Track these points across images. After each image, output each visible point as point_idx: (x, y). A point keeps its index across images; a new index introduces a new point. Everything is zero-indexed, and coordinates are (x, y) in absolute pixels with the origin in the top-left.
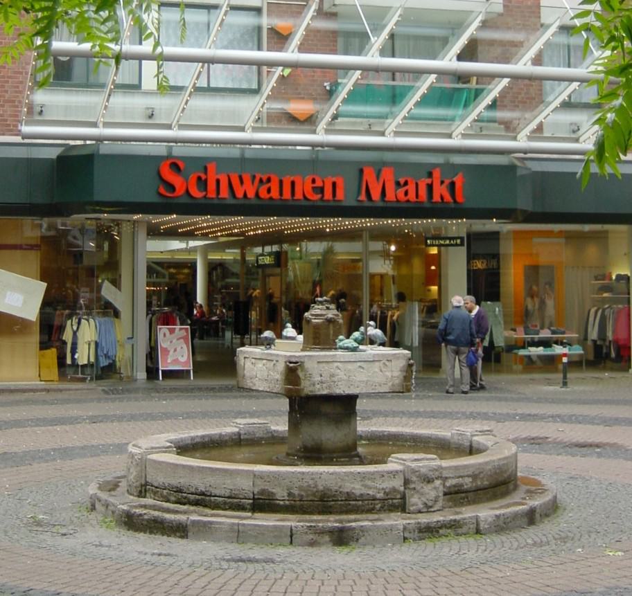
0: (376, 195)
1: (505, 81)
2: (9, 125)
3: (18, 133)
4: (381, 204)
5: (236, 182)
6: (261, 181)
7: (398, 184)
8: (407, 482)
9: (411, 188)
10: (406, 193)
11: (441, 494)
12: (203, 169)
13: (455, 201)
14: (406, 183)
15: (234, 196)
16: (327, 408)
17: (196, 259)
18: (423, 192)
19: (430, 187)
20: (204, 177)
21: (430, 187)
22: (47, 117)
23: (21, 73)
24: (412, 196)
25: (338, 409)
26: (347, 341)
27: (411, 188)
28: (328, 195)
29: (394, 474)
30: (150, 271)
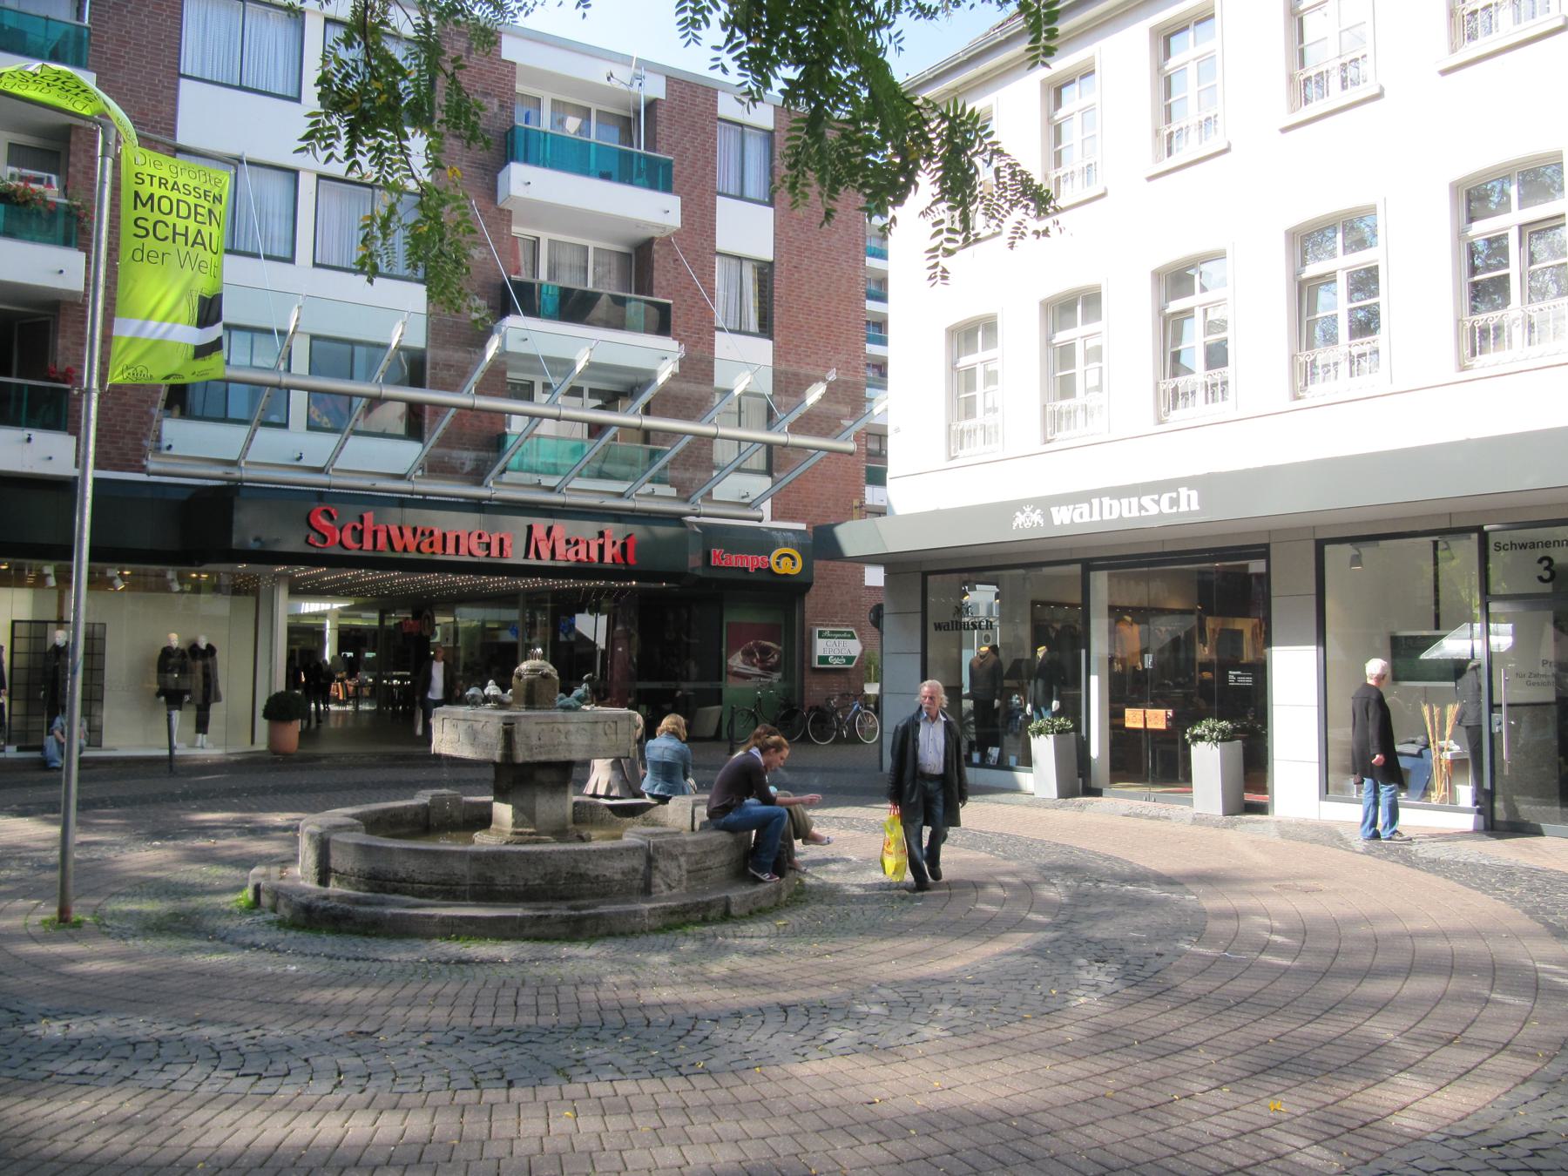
0: (546, 554)
1: (688, 438)
2: (129, 460)
3: (142, 469)
4: (551, 563)
5: (395, 533)
6: (423, 534)
7: (568, 542)
8: (650, 860)
9: (582, 548)
10: (577, 553)
11: (684, 873)
12: (358, 519)
13: (626, 563)
14: (577, 542)
15: (392, 549)
16: (541, 775)
17: (324, 626)
18: (594, 554)
19: (601, 548)
20: (359, 527)
21: (601, 548)
22: (174, 452)
23: (146, 402)
24: (582, 556)
25: (554, 776)
26: (567, 699)
27: (582, 548)
28: (495, 551)
29: (631, 850)
30: (292, 630)
